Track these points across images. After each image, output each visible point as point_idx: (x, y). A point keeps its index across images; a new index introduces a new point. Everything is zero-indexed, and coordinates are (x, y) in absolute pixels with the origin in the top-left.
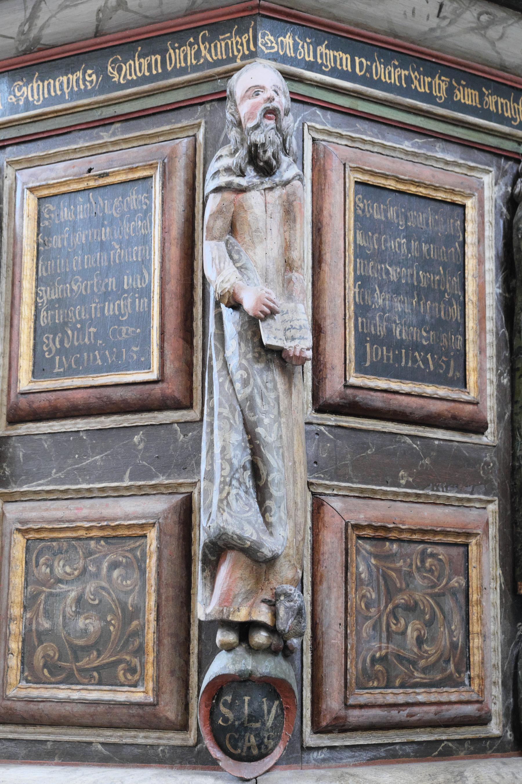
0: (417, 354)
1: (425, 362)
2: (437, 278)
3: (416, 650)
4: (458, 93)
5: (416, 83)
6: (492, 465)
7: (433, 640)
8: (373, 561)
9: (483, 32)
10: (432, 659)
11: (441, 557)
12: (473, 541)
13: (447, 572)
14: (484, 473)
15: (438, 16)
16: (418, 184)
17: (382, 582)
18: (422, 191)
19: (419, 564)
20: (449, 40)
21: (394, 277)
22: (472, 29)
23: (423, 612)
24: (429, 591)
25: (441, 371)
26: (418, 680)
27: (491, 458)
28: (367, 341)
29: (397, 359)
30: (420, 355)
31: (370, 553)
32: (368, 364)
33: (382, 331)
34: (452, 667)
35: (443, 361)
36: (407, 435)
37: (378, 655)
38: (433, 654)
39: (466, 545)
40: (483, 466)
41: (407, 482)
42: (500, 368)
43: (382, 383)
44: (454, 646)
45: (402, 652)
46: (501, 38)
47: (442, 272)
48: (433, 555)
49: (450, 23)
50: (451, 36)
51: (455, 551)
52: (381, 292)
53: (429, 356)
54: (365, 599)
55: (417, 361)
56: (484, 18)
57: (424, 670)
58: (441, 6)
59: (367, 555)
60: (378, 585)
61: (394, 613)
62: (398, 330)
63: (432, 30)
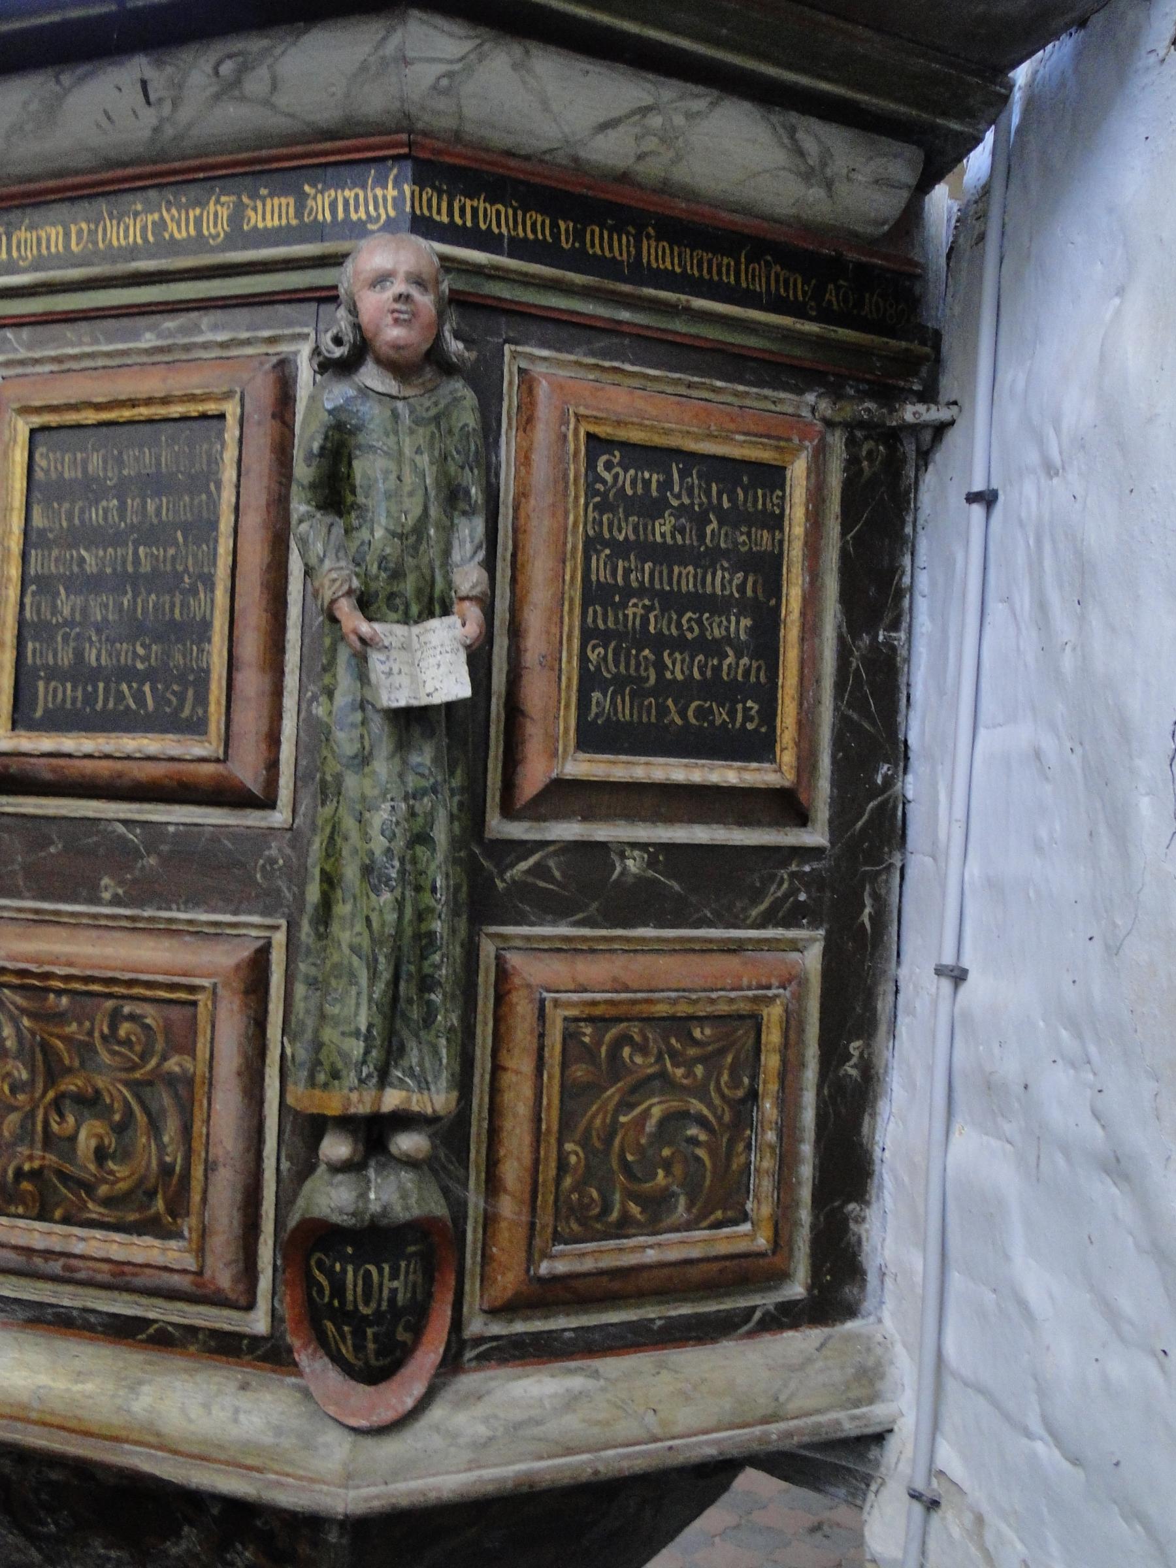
0: (124, 687)
1: (140, 698)
2: (171, 551)
3: (92, 1167)
4: (252, 214)
5: (172, 227)
6: (281, 862)
7: (125, 1155)
8: (26, 1022)
9: (237, 93)
10: (122, 1186)
11: (148, 1021)
12: (200, 997)
13: (160, 1046)
14: (263, 877)
15: (148, 103)
16: (133, 403)
17: (39, 1056)
18: (144, 412)
19: (106, 1030)
20: (195, 132)
21: (91, 565)
22: (217, 97)
23: (110, 1109)
24: (123, 1075)
25: (168, 710)
26: (94, 1216)
27: (280, 850)
28: (40, 678)
29: (90, 699)
30: (130, 687)
31: (23, 1011)
32: (39, 714)
33: (65, 658)
34: (160, 1205)
35: (174, 693)
36: (119, 820)
37: (27, 1167)
38: (124, 1179)
39: (194, 1004)
40: (263, 866)
41: (116, 895)
42: (312, 687)
43: (47, 743)
44: (166, 1170)
45: (69, 1168)
46: (274, 87)
47: (181, 539)
48: (132, 1017)
49: (175, 105)
50: (190, 125)
51: (175, 1013)
52: (68, 597)
53: (147, 688)
54: (8, 1080)
55: (124, 698)
56: (227, 68)
57: (108, 1202)
58: (144, 84)
59: (16, 1012)
60: (33, 1059)
61: (57, 1105)
62: (94, 651)
63: (156, 130)
